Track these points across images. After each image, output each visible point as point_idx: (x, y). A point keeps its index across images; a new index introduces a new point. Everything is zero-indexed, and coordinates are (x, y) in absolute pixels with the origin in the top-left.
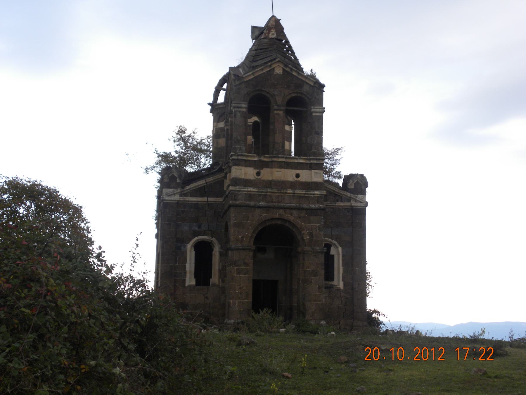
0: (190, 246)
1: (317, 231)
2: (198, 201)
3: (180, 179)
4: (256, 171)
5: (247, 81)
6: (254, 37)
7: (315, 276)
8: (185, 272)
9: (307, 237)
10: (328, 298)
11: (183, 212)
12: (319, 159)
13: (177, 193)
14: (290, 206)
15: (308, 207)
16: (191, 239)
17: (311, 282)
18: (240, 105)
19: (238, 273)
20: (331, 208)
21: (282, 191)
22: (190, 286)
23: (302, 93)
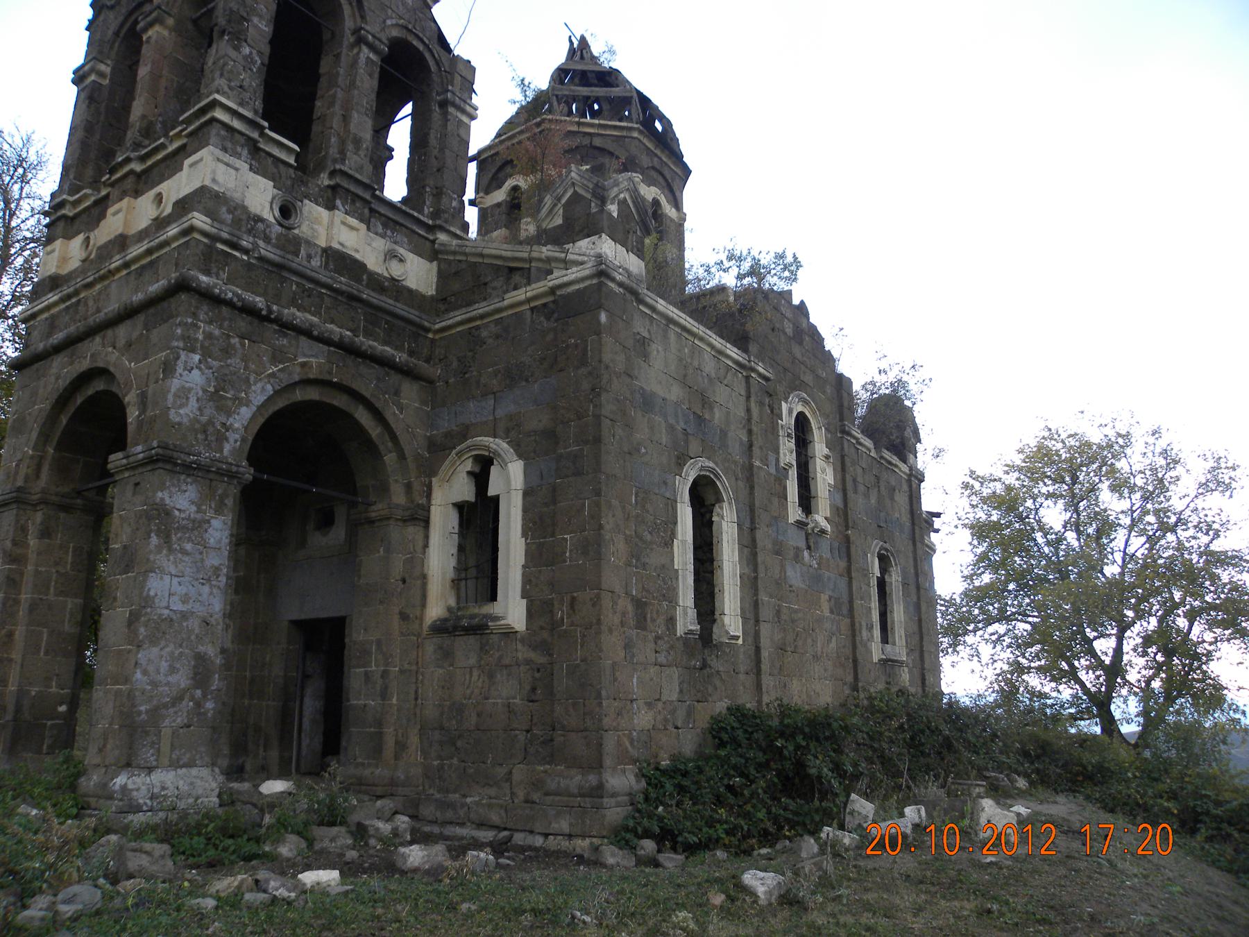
9: (132, 415)
10: (475, 673)
20: (497, 322)
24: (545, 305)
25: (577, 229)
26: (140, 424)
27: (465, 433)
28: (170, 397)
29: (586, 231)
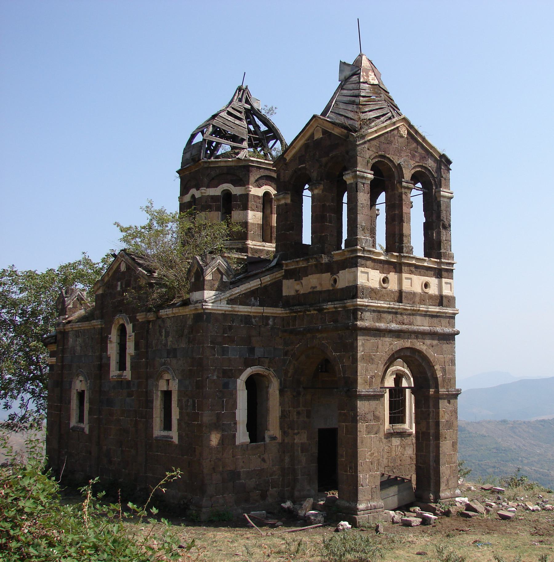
0: (241, 382)
2: (250, 312)
3: (228, 276)
4: (383, 276)
6: (343, 77)
7: (449, 428)
8: (235, 424)
9: (439, 374)
10: (399, 447)
11: (230, 328)
12: (450, 264)
13: (224, 298)
14: (424, 330)
15: (442, 332)
16: (241, 372)
17: (445, 438)
18: (365, 175)
19: (369, 433)
21: (415, 308)
22: (242, 445)
23: (426, 168)
26: (444, 380)
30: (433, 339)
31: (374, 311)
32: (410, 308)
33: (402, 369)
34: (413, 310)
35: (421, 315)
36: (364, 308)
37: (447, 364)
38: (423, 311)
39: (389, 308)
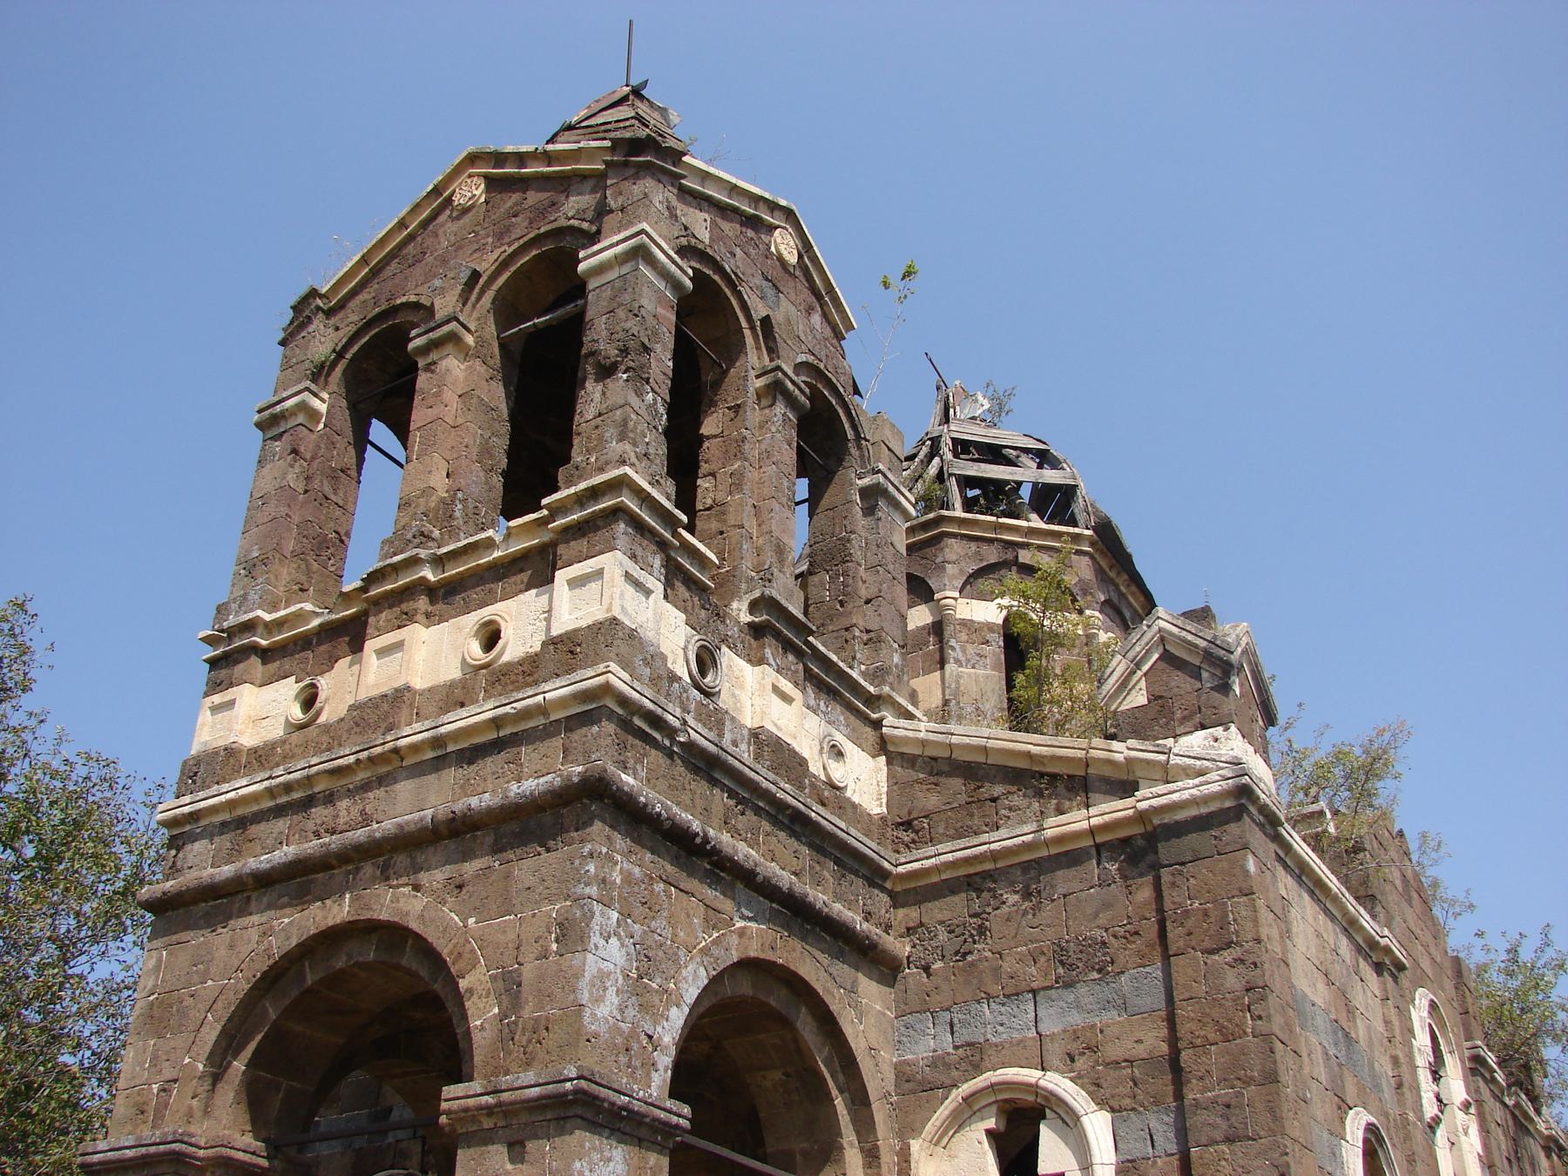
1: (544, 955)
5: (342, 305)
9: (482, 1015)
14: (407, 823)
21: (379, 750)
24: (1126, 841)
25: (1178, 714)
26: (507, 1033)
27: (975, 1057)
28: (583, 984)
29: (1198, 718)
30: (466, 856)
31: (224, 827)
32: (352, 759)
33: (1031, 1075)
34: (371, 760)
35: (420, 770)
36: (188, 828)
37: (529, 955)
38: (415, 748)
39: (270, 792)
